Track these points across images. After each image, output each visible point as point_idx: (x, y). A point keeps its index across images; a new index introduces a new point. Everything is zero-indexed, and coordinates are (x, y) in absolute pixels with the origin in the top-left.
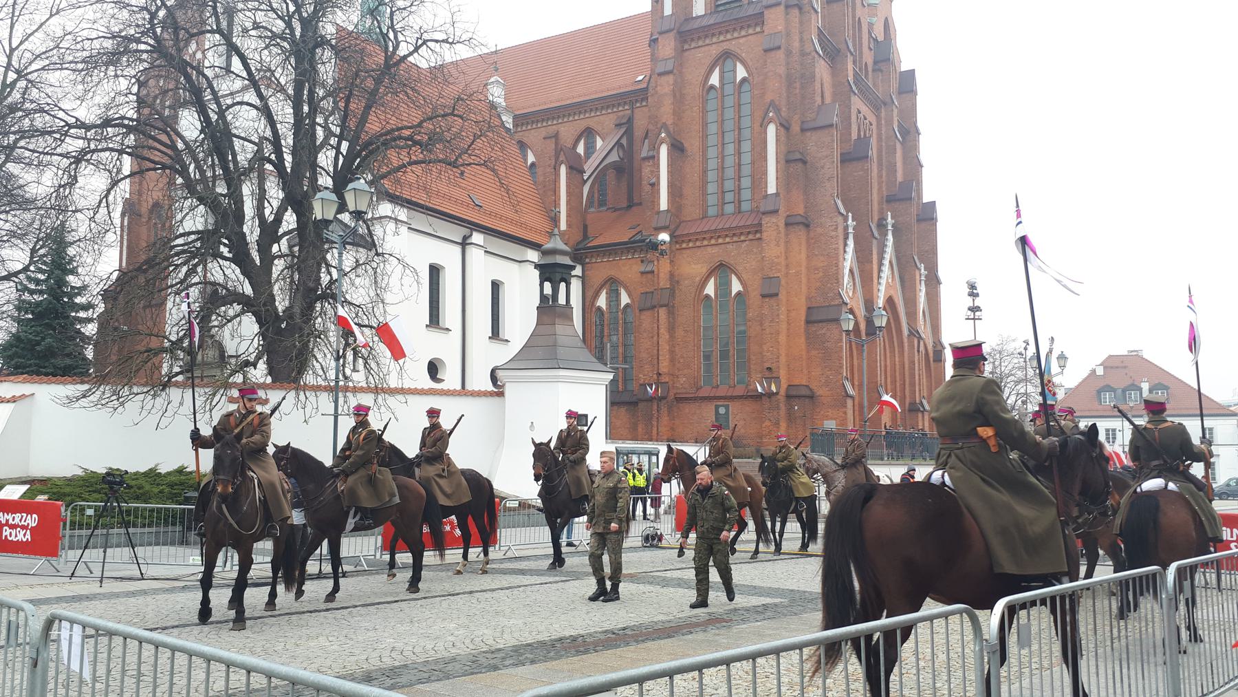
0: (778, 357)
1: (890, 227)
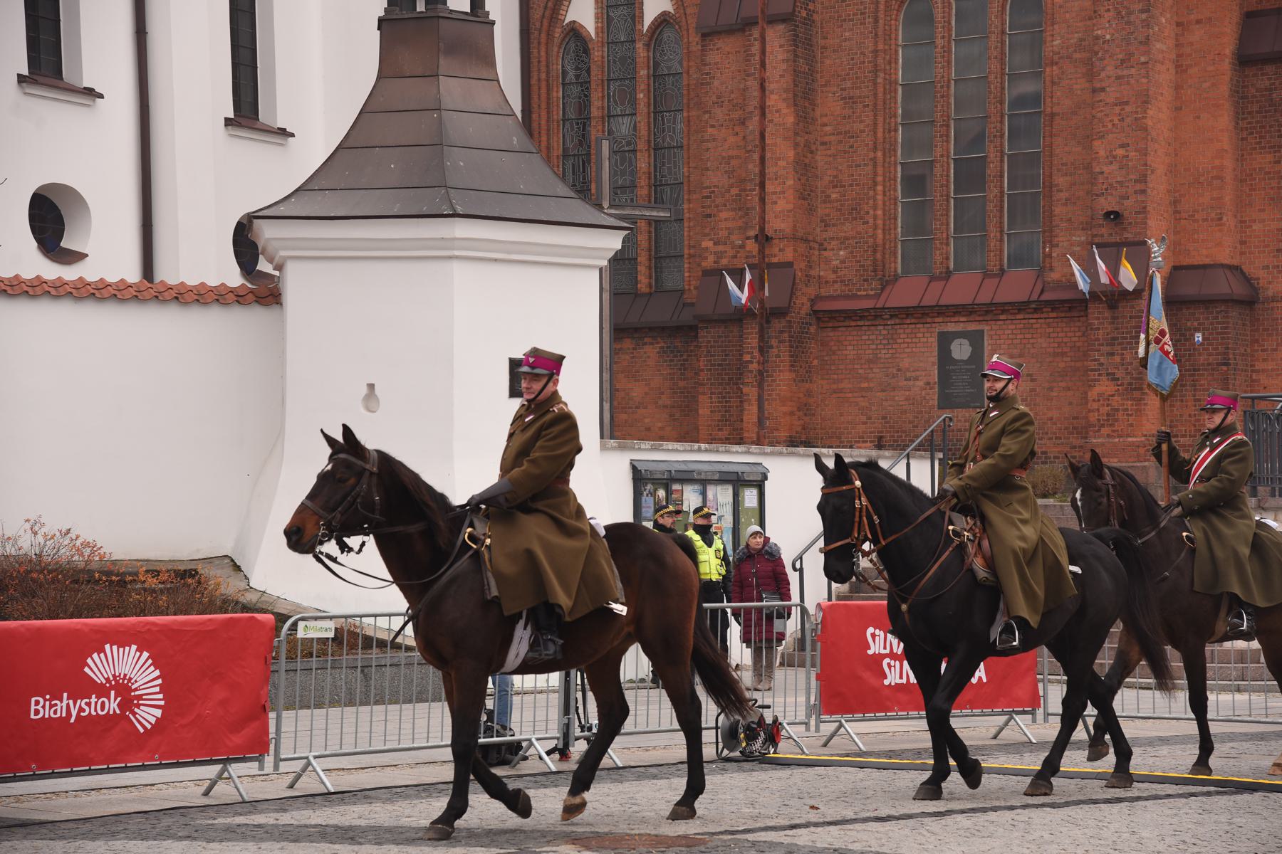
0: (1143, 179)
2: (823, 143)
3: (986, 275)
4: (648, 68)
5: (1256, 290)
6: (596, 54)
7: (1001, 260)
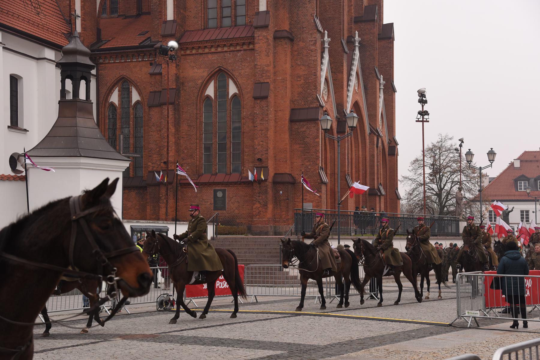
0: (267, 150)
1: (357, 44)
2: (183, 137)
3: (226, 174)
4: (133, 115)
5: (295, 180)
6: (118, 111)
7: (230, 170)
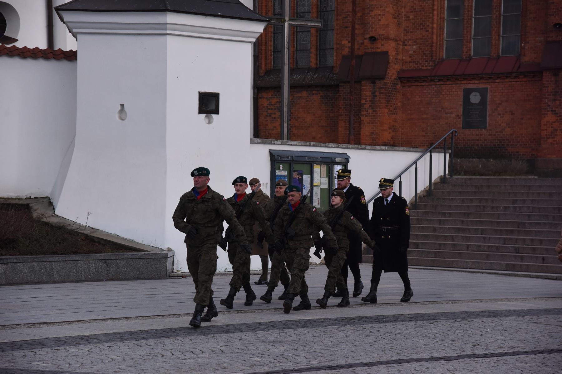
7: (498, 50)
